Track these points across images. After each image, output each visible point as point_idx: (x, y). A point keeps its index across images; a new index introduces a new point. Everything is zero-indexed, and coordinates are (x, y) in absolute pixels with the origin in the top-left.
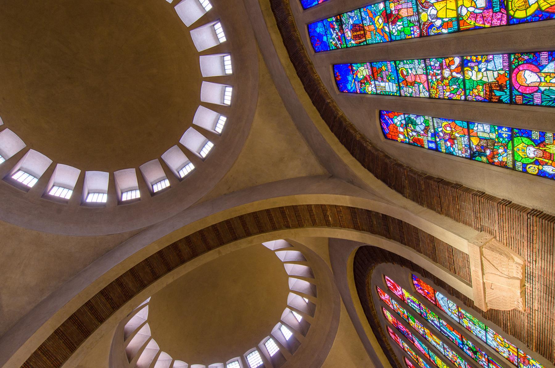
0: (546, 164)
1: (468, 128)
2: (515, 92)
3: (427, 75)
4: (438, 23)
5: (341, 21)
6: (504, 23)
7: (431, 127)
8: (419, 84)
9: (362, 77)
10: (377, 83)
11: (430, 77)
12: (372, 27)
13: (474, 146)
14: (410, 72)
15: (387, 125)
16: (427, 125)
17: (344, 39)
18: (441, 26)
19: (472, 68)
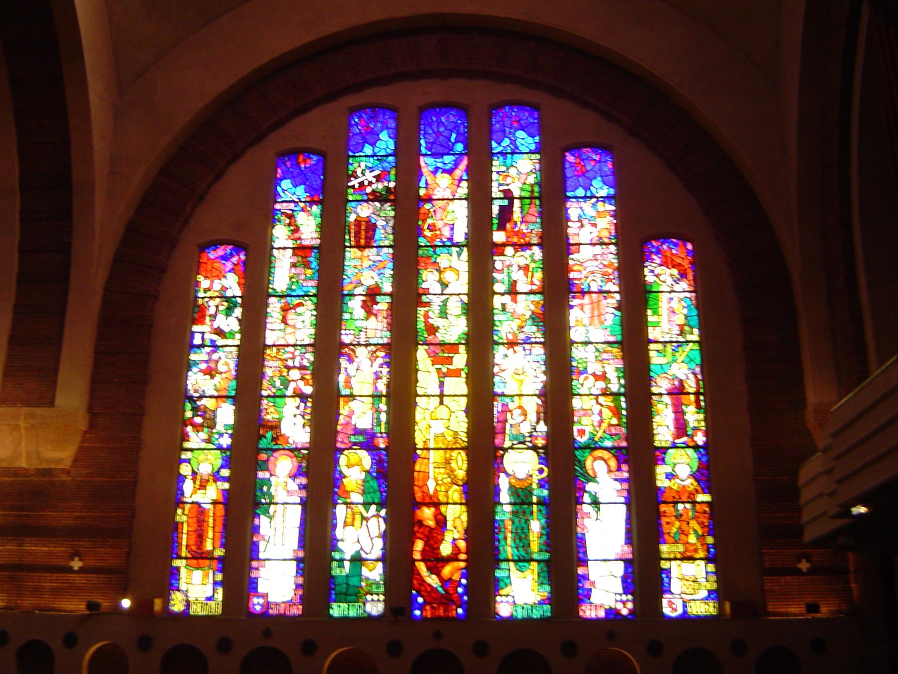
1: (227, 397)
2: (270, 453)
3: (293, 346)
5: (386, 201)
6: (339, 445)
11: (291, 349)
16: (227, 335)
17: (359, 198)
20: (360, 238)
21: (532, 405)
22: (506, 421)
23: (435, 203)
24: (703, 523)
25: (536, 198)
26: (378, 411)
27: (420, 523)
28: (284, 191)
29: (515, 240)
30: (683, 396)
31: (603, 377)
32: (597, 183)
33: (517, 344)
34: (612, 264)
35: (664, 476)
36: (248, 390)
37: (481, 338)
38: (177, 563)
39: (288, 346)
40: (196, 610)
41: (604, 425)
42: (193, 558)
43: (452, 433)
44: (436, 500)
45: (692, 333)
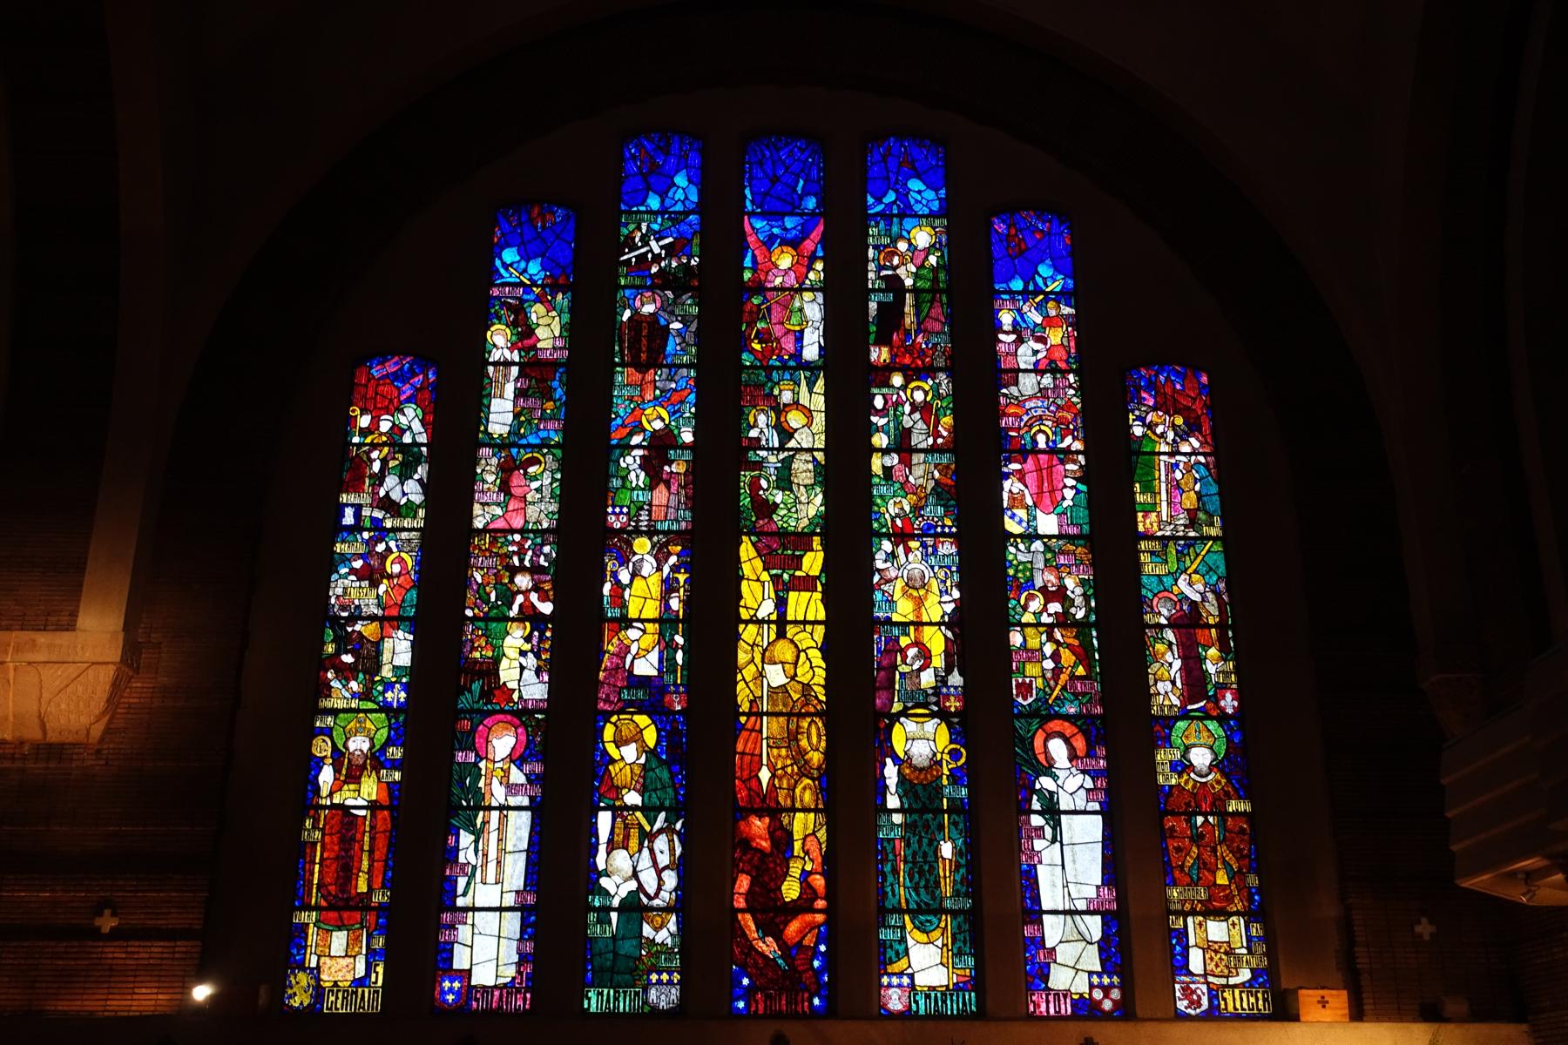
0: (337, 771)
2: (477, 719)
3: (521, 531)
4: (624, 576)
7: (397, 523)
8: (504, 505)
9: (534, 317)
10: (515, 370)
11: (517, 537)
12: (648, 397)
13: (358, 627)
14: (535, 485)
15: (395, 377)
16: (403, 511)
17: (638, 282)
18: (618, 582)
19: (528, 639)
20: (640, 351)
21: (936, 641)
22: (896, 667)
23: (769, 294)
24: (1240, 850)
25: (941, 291)
26: (670, 647)
27: (746, 843)
28: (506, 266)
29: (907, 360)
30: (1199, 632)
31: (1060, 594)
32: (1045, 270)
33: (913, 537)
34: (1075, 405)
35: (1167, 768)
36: (440, 607)
37: (849, 530)
38: (304, 917)
39: (513, 531)
40: (335, 1004)
41: (1064, 678)
42: (330, 908)
43: (800, 687)
44: (773, 805)
45: (1212, 524)
